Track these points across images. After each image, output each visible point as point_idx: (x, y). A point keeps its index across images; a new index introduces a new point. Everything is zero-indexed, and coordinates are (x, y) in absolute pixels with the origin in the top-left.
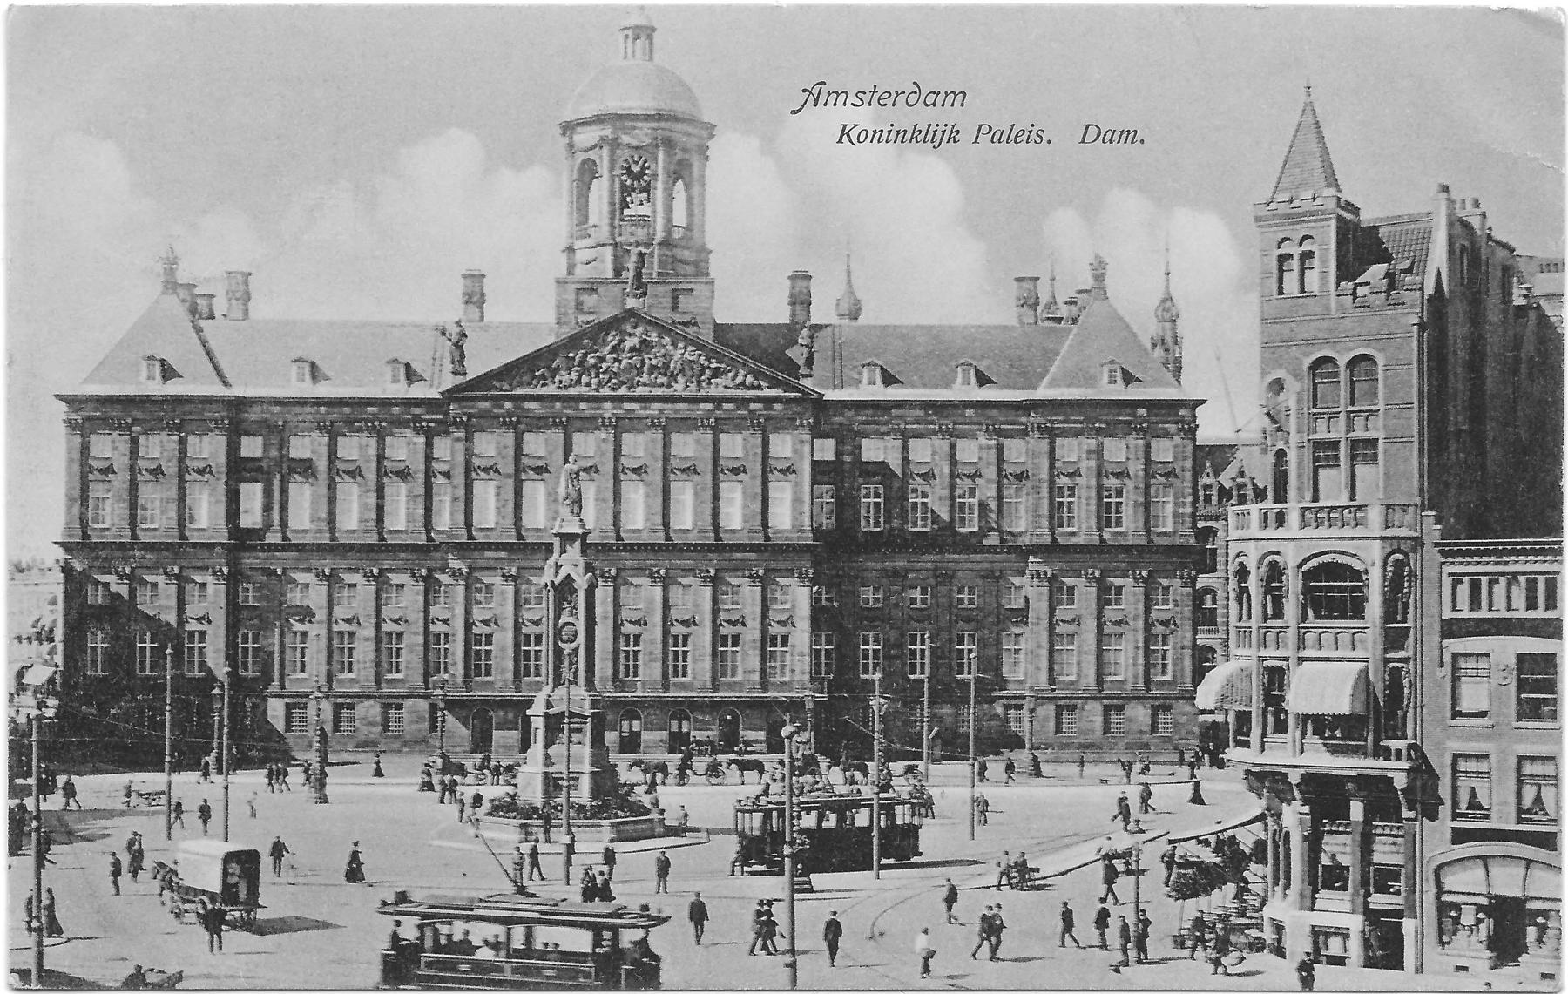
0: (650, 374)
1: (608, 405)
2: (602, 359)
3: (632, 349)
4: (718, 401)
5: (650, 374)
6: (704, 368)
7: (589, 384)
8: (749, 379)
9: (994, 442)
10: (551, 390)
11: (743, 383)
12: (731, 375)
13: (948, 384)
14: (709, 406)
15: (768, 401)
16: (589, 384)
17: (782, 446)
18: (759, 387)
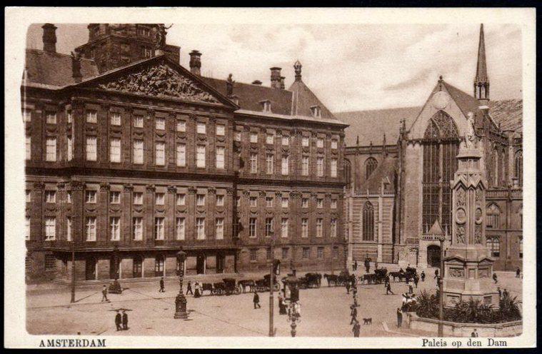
0: (171, 89)
1: (151, 103)
2: (149, 79)
3: (163, 75)
4: (197, 106)
5: (171, 89)
6: (193, 89)
7: (144, 91)
8: (211, 97)
9: (279, 136)
10: (125, 91)
11: (207, 100)
12: (202, 94)
13: (260, 110)
14: (194, 108)
15: (217, 109)
16: (144, 91)
17: (221, 131)
18: (213, 101)
